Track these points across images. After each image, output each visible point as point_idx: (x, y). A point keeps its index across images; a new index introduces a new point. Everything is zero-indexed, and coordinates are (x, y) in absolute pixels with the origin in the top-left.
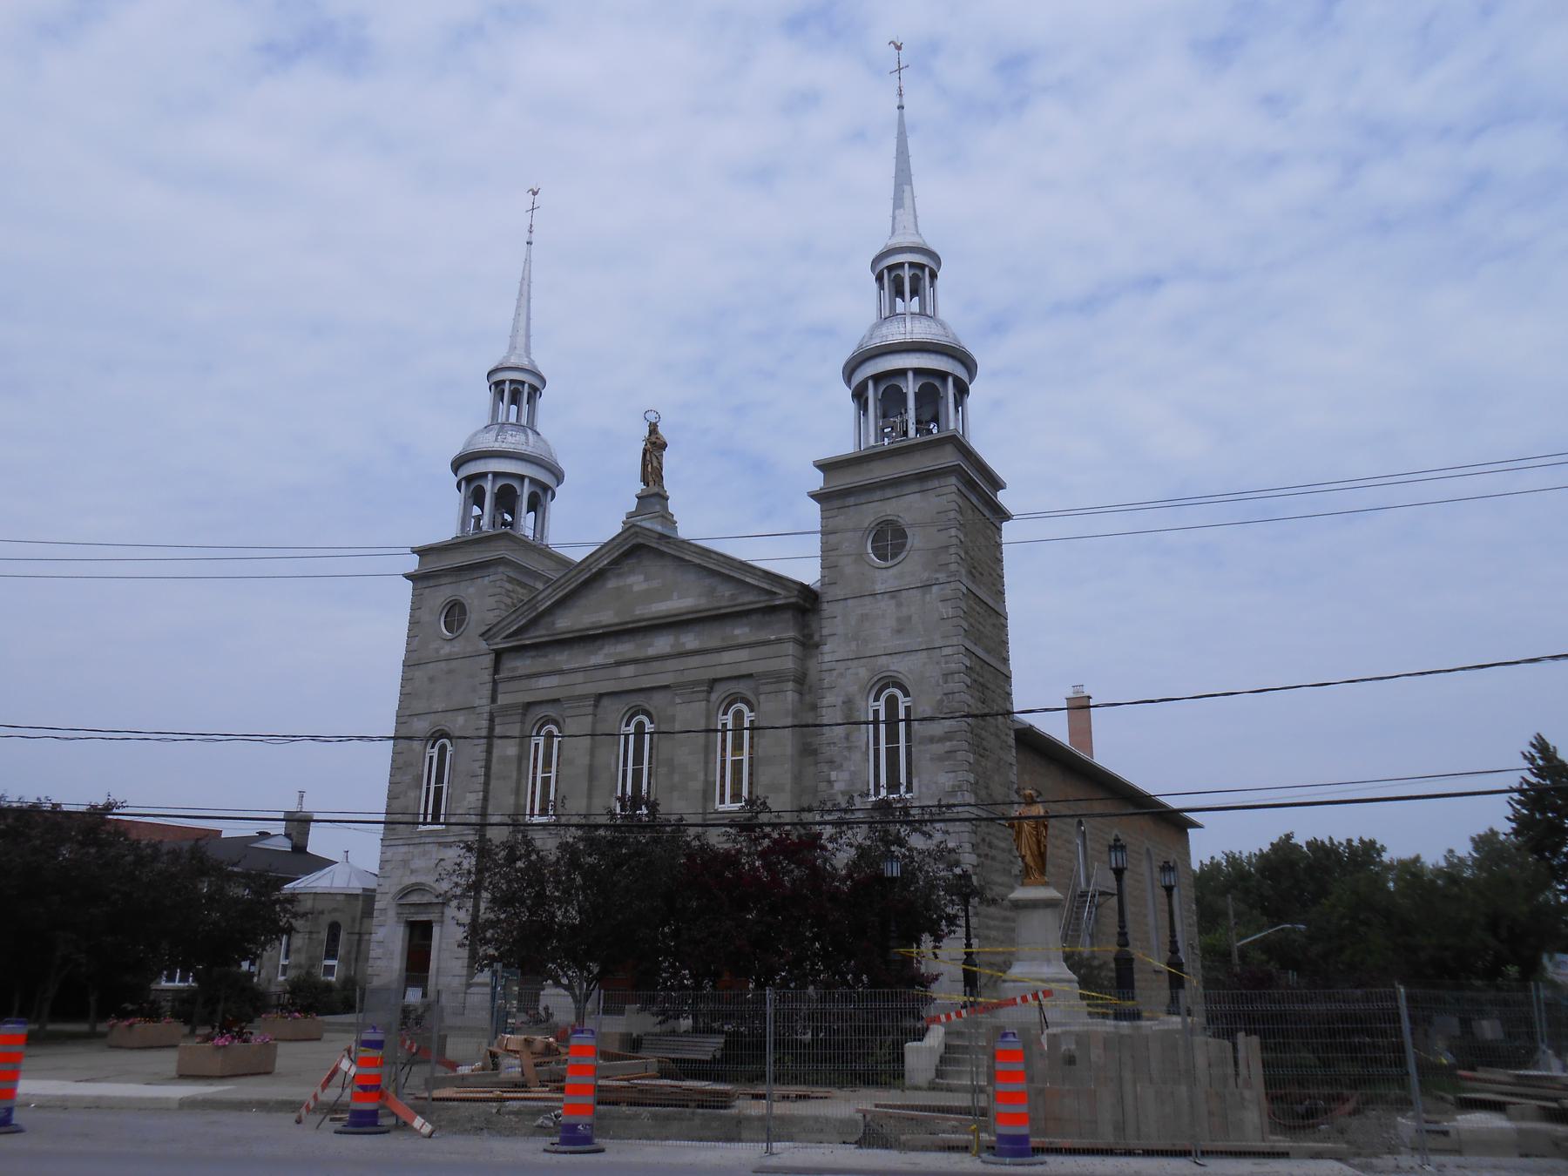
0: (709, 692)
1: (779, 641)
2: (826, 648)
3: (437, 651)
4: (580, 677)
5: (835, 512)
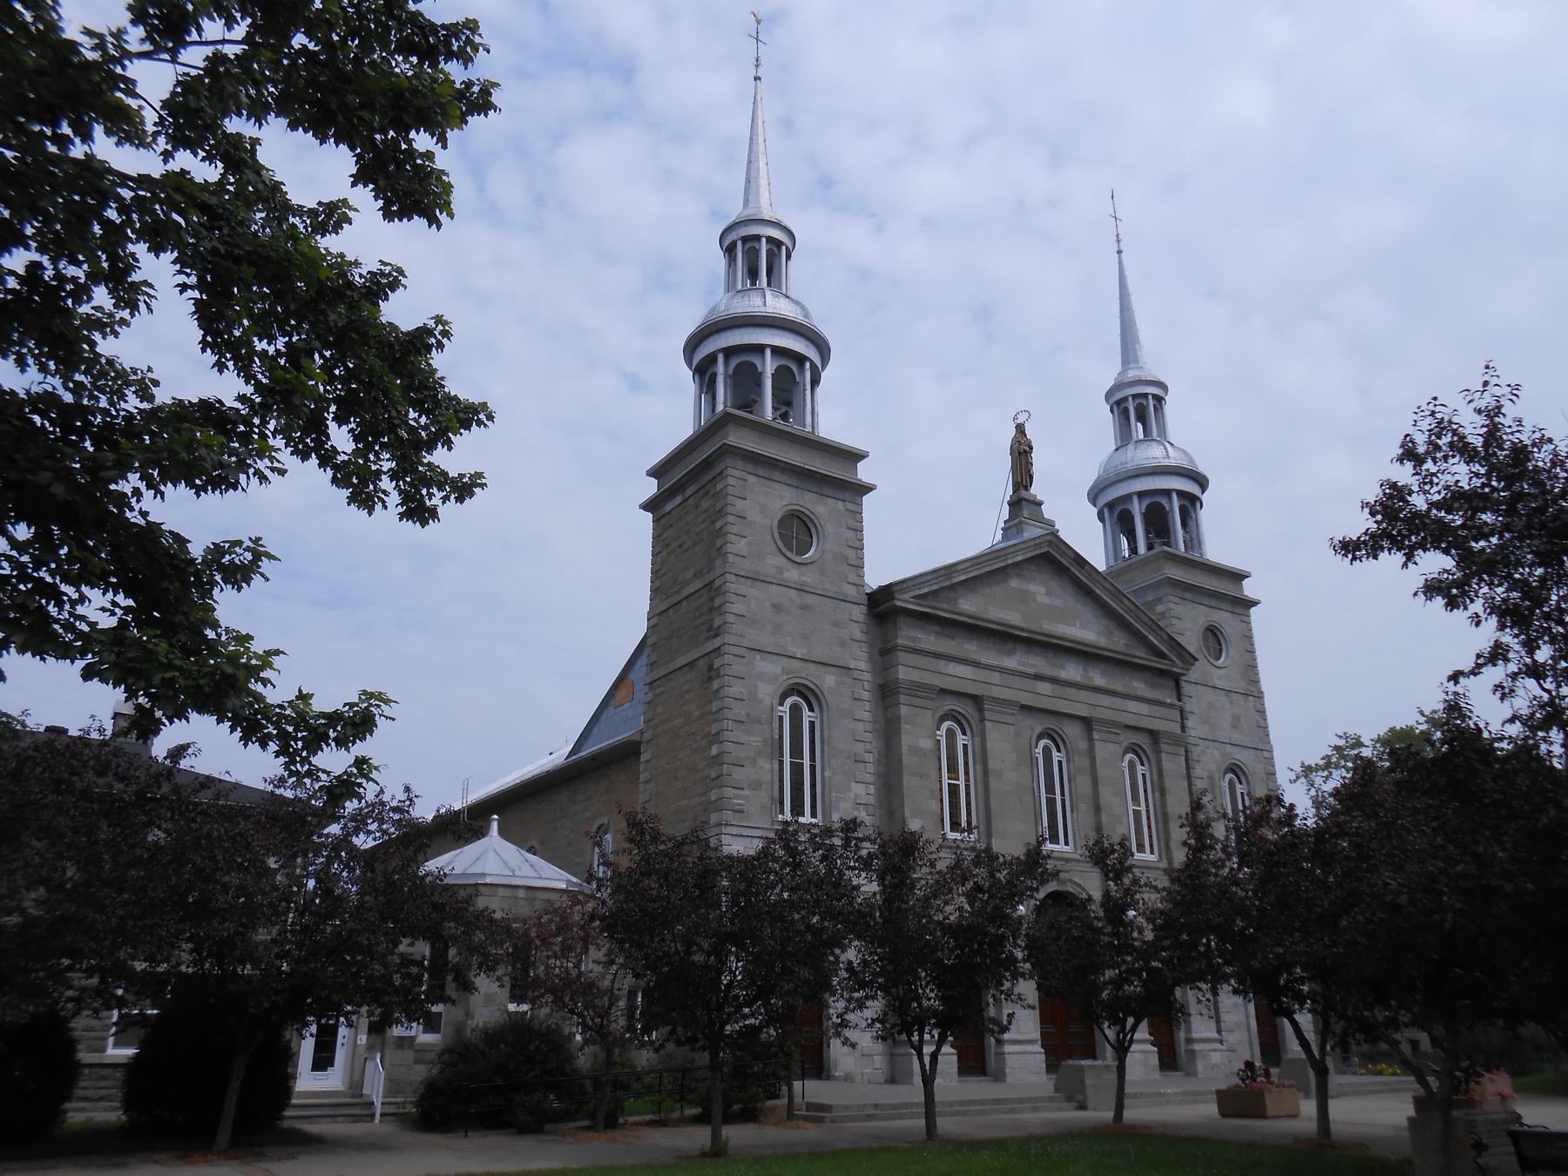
3: (780, 571)
4: (995, 677)
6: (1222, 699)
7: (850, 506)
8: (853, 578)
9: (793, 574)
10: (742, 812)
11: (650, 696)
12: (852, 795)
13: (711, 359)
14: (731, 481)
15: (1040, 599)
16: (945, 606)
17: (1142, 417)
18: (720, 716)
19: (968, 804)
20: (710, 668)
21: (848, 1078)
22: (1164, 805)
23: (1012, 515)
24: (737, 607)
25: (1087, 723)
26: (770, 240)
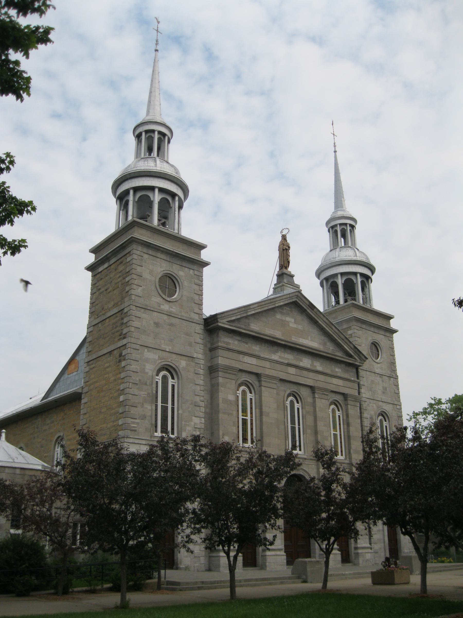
3: (159, 305)
4: (268, 364)
5: (359, 328)
6: (378, 379)
7: (196, 273)
8: (197, 310)
9: (166, 307)
10: (135, 431)
11: (87, 369)
12: (193, 423)
13: (126, 192)
14: (135, 257)
15: (291, 325)
16: (244, 327)
17: (344, 235)
18: (125, 380)
19: (252, 429)
20: (121, 355)
21: (187, 568)
22: (348, 431)
23: (279, 281)
24: (136, 323)
25: (312, 388)
26: (160, 133)
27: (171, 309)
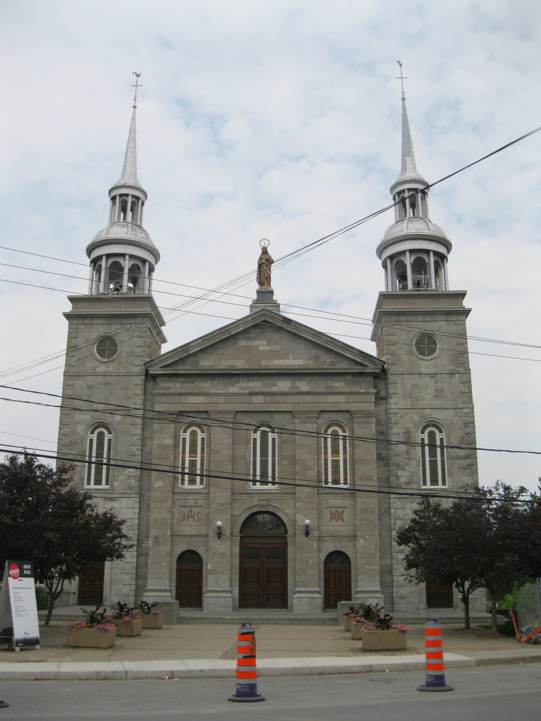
0: (318, 418)
1: (366, 393)
2: (392, 401)
3: (94, 368)
4: (222, 399)
6: (427, 380)
27: (107, 369)
